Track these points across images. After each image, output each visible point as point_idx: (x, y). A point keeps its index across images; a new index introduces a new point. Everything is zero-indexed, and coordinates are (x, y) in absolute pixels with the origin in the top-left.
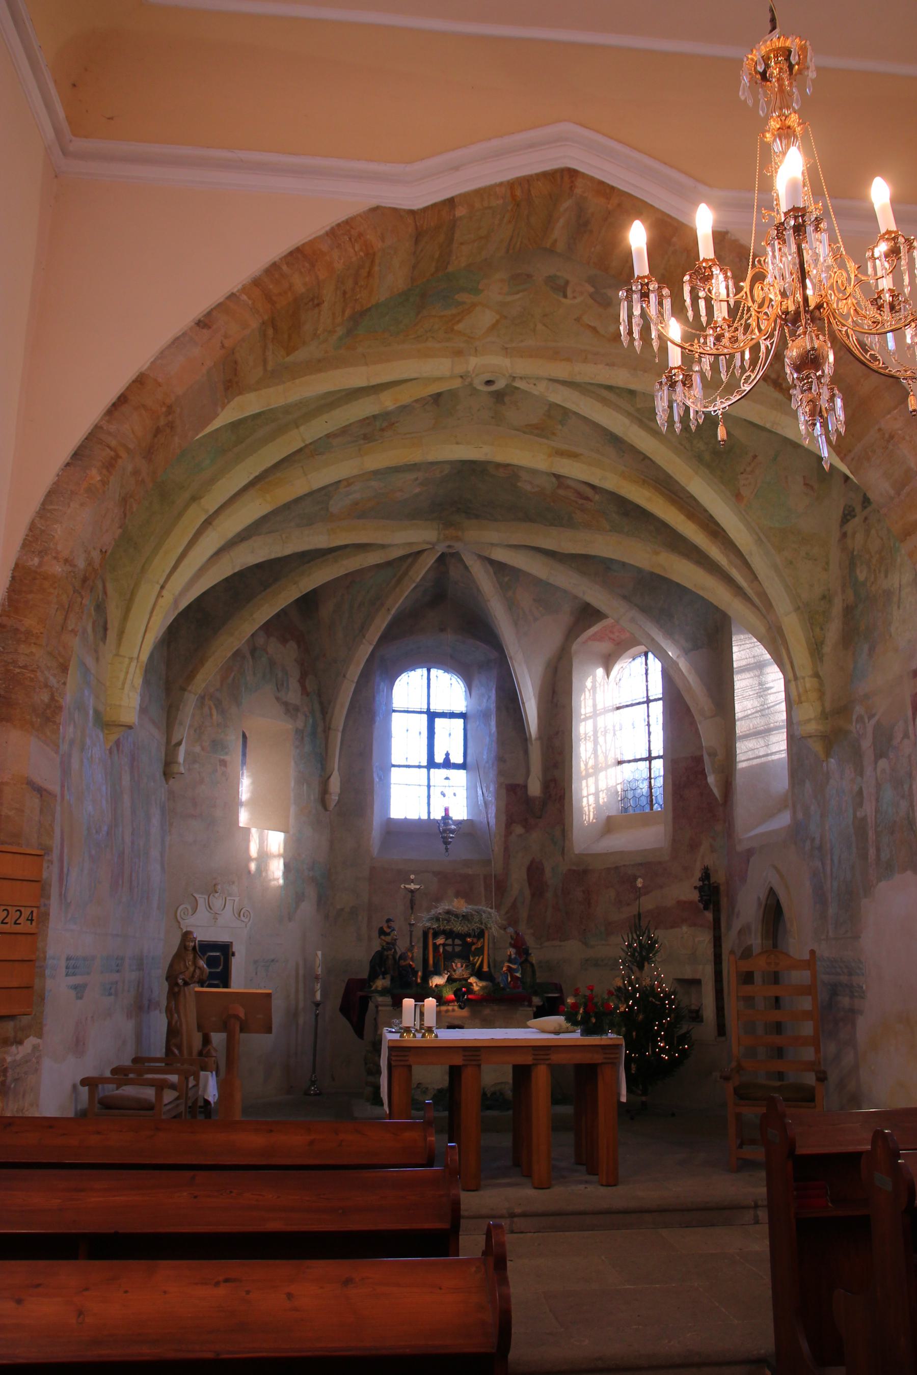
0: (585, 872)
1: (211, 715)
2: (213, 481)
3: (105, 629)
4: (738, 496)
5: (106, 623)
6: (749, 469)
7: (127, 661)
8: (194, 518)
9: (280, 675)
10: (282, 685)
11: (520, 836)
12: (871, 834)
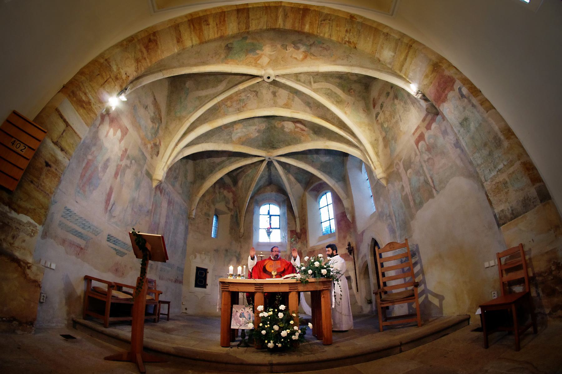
0: (314, 251)
12: (410, 198)
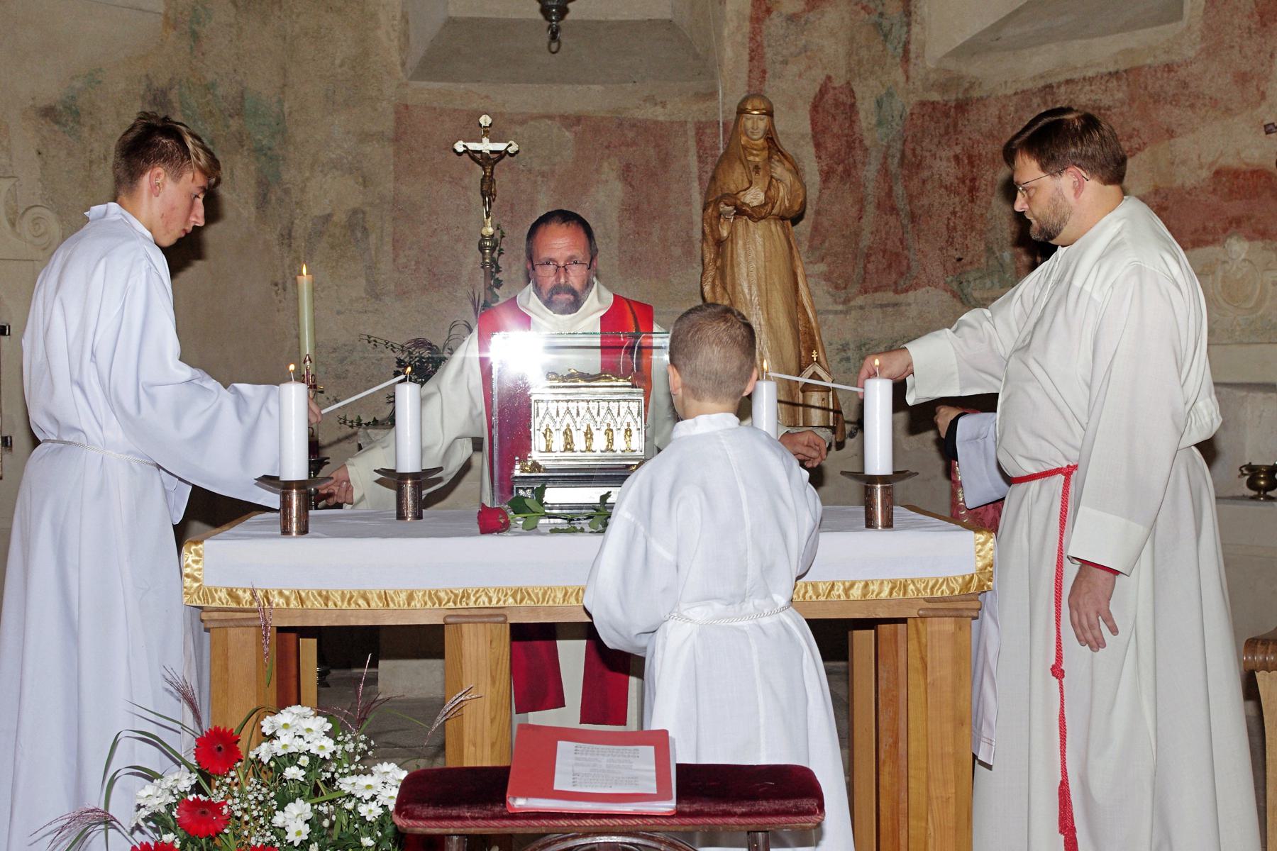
0: (962, 107)
11: (792, 18)
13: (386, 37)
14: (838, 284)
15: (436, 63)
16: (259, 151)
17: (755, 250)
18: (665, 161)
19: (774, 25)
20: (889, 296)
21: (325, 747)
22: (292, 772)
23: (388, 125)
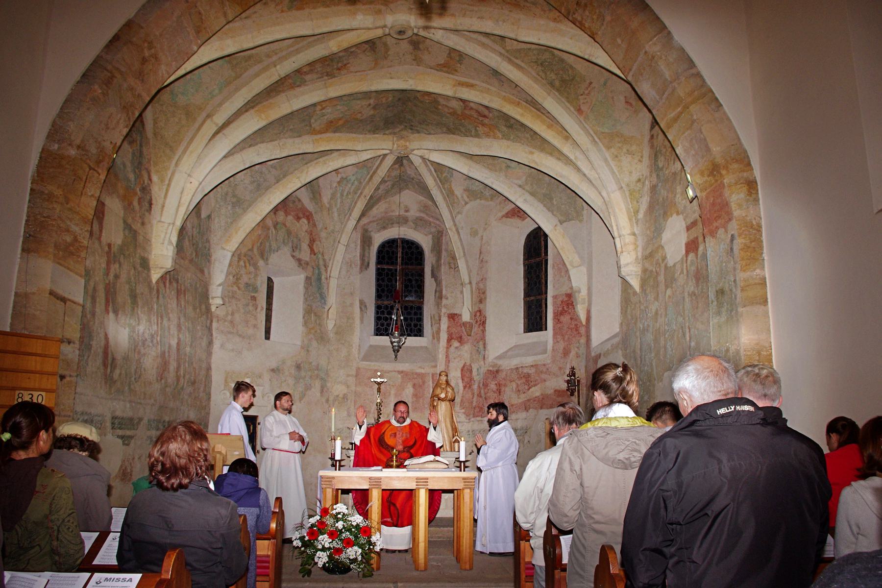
0: (497, 371)
1: (245, 266)
2: (220, 105)
3: (151, 204)
4: (579, 111)
5: (151, 200)
6: (586, 92)
7: (166, 225)
8: (209, 128)
9: (295, 240)
10: (296, 248)
11: (456, 348)
13: (355, 351)
14: (467, 415)
15: (366, 358)
16: (322, 379)
17: (443, 407)
18: (424, 382)
19: (452, 349)
20: (479, 418)
21: (346, 512)
22: (340, 516)
23: (354, 373)
